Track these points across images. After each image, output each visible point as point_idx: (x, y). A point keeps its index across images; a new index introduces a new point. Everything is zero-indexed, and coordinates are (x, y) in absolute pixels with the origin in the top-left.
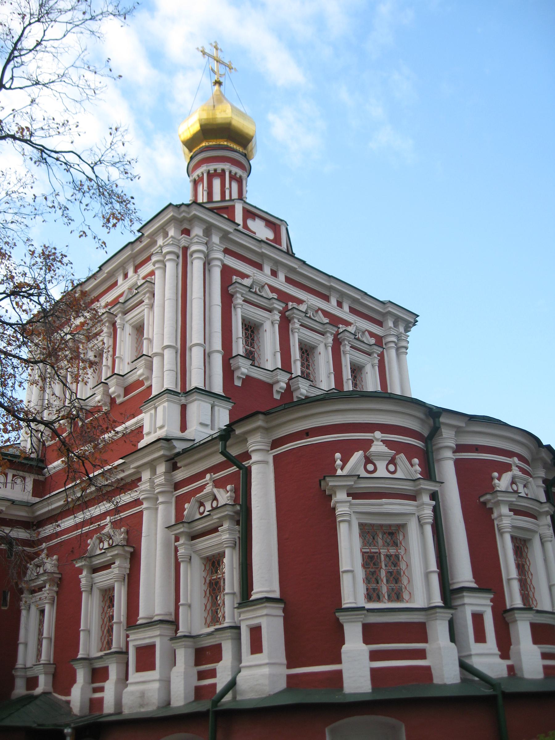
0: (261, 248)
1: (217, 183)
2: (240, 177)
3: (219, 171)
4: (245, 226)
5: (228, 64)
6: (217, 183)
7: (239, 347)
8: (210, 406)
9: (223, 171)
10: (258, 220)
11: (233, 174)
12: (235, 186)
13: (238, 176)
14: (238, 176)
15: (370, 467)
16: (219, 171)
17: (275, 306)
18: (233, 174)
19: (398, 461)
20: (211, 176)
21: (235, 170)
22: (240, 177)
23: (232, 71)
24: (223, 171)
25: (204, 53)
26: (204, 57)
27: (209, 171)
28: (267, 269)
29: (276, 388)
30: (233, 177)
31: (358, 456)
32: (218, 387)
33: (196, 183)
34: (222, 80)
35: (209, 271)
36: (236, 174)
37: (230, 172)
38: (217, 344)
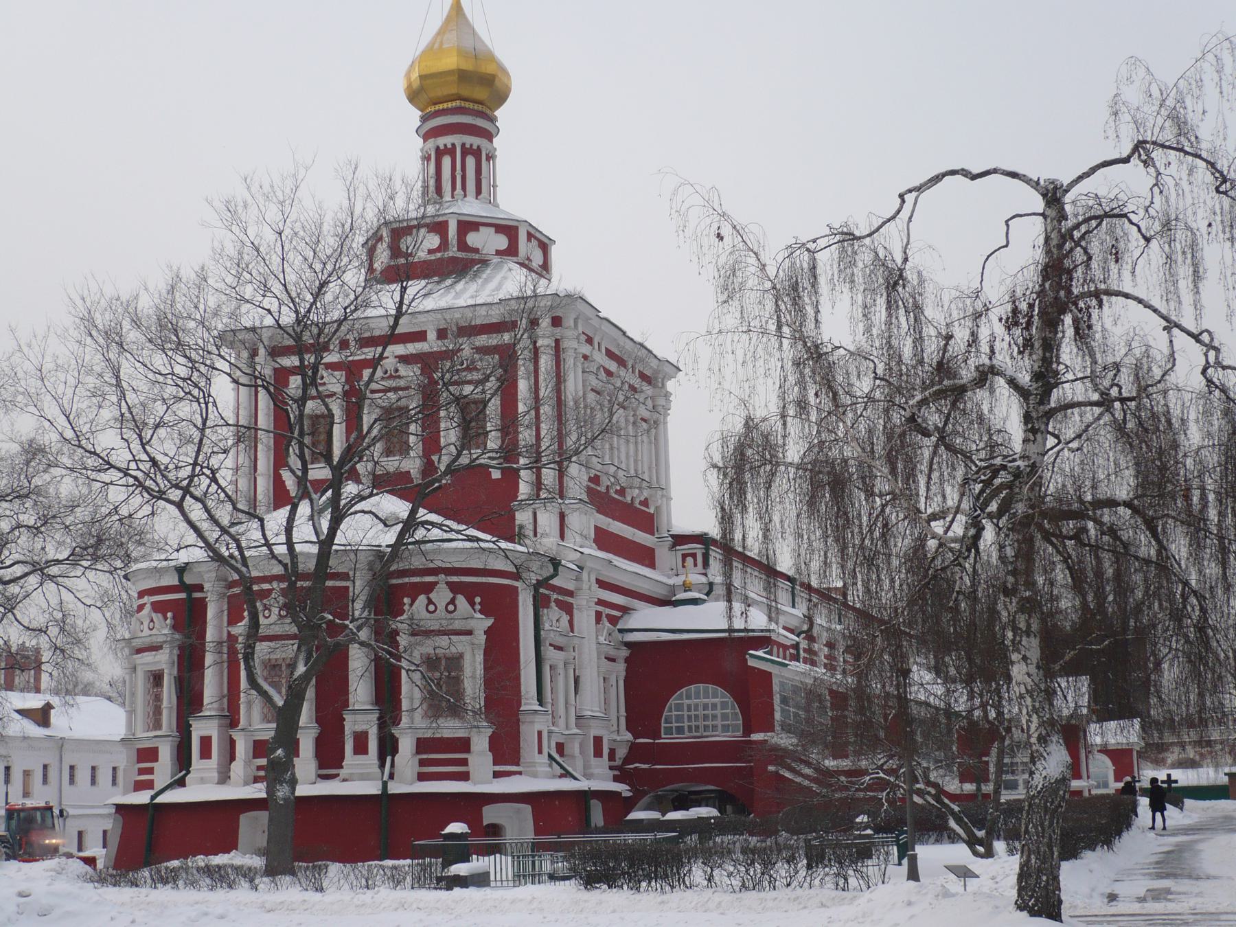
2: (478, 147)
3: (449, 146)
4: (463, 245)
6: (447, 161)
9: (453, 145)
10: (481, 228)
11: (468, 146)
12: (471, 161)
13: (475, 147)
14: (475, 147)
15: (431, 608)
16: (449, 146)
18: (468, 146)
19: (457, 602)
20: (440, 153)
24: (453, 145)
27: (438, 148)
30: (466, 151)
31: (422, 599)
33: (427, 158)
36: (471, 145)
37: (463, 145)
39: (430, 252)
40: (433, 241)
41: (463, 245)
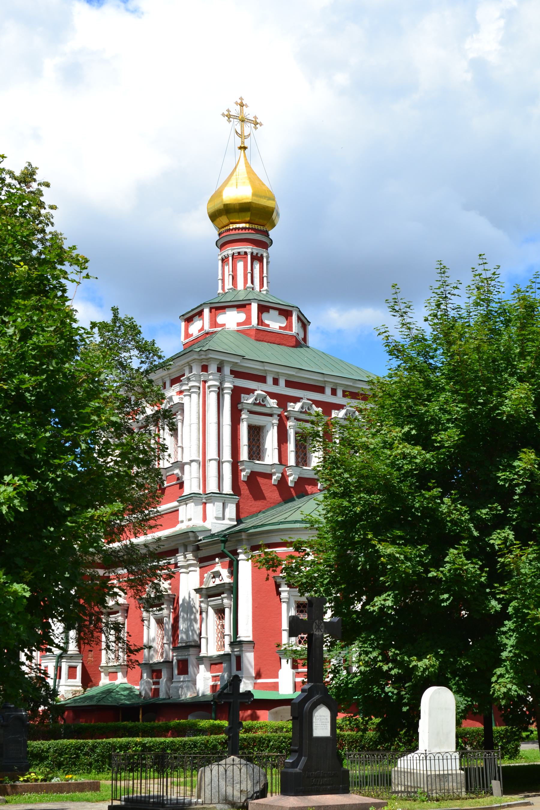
0: (264, 366)
1: (240, 265)
5: (254, 119)
6: (240, 265)
7: (244, 455)
8: (221, 504)
10: (271, 311)
11: (255, 254)
13: (259, 255)
14: (259, 255)
17: (275, 412)
18: (255, 254)
21: (256, 250)
22: (262, 255)
23: (258, 126)
25: (229, 116)
26: (230, 121)
28: (270, 380)
29: (274, 477)
32: (227, 488)
34: (246, 145)
35: (223, 395)
36: (257, 254)
37: (252, 253)
38: (227, 455)
39: (239, 324)
40: (241, 317)
41: (260, 322)
